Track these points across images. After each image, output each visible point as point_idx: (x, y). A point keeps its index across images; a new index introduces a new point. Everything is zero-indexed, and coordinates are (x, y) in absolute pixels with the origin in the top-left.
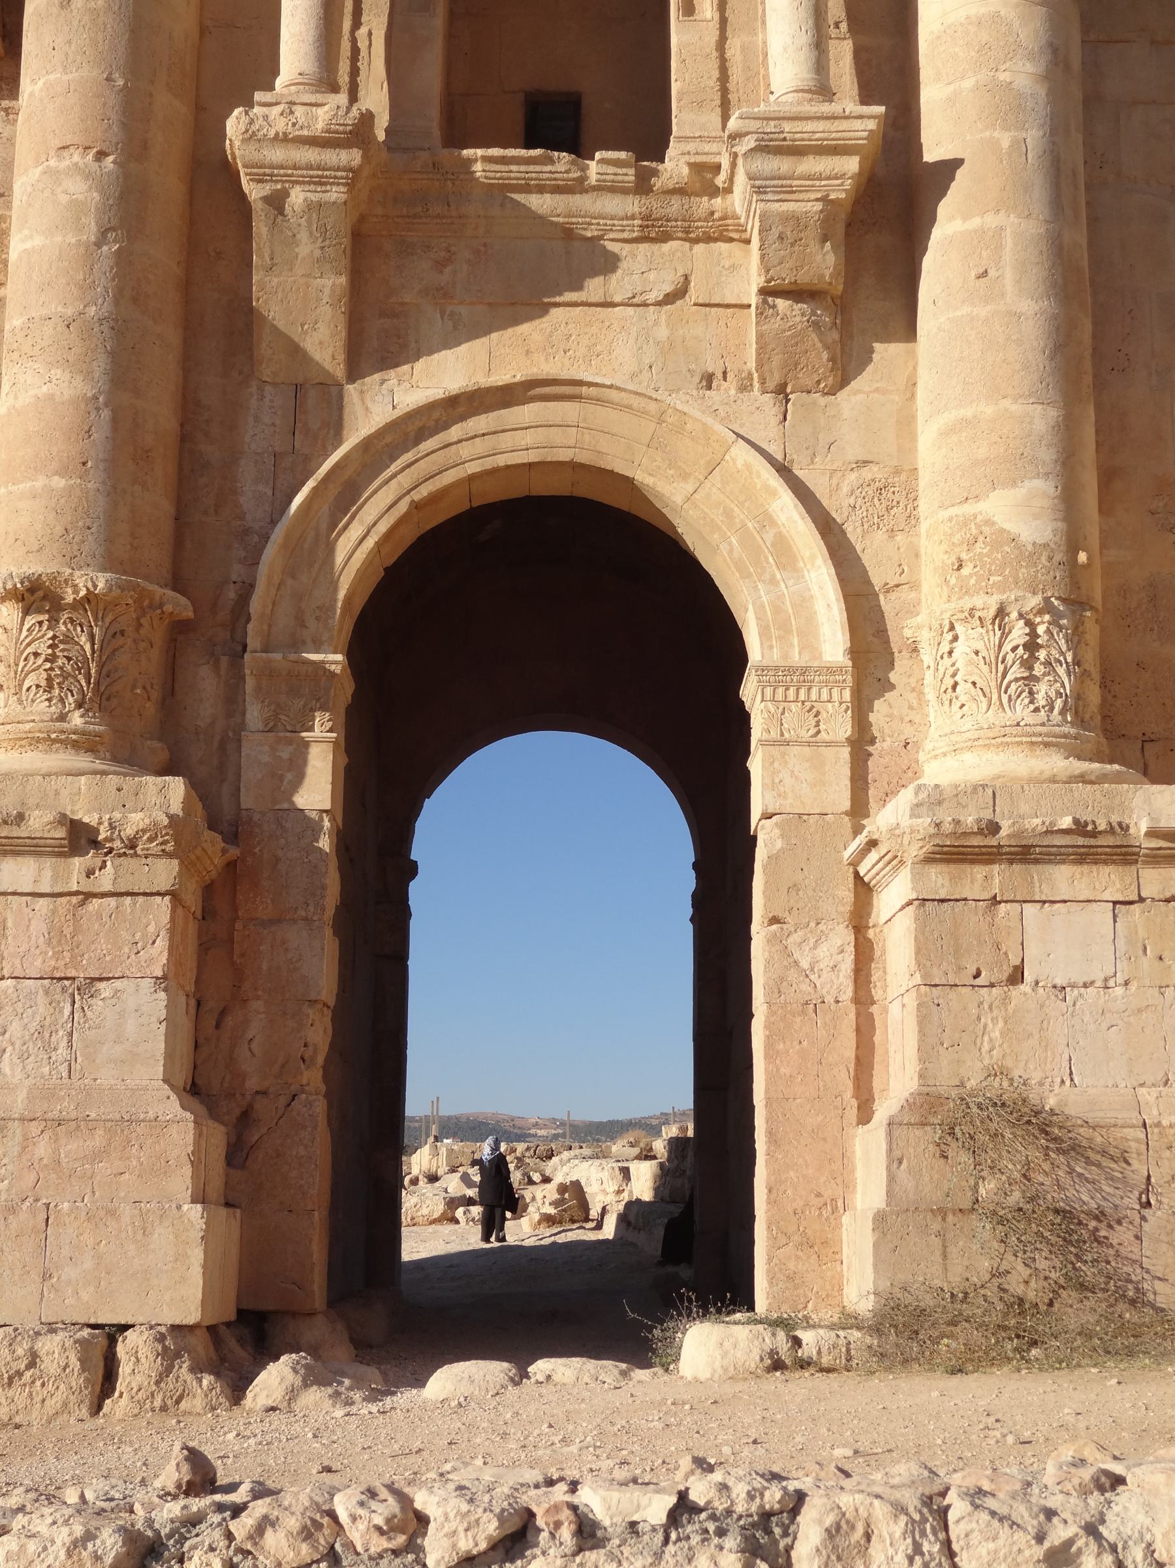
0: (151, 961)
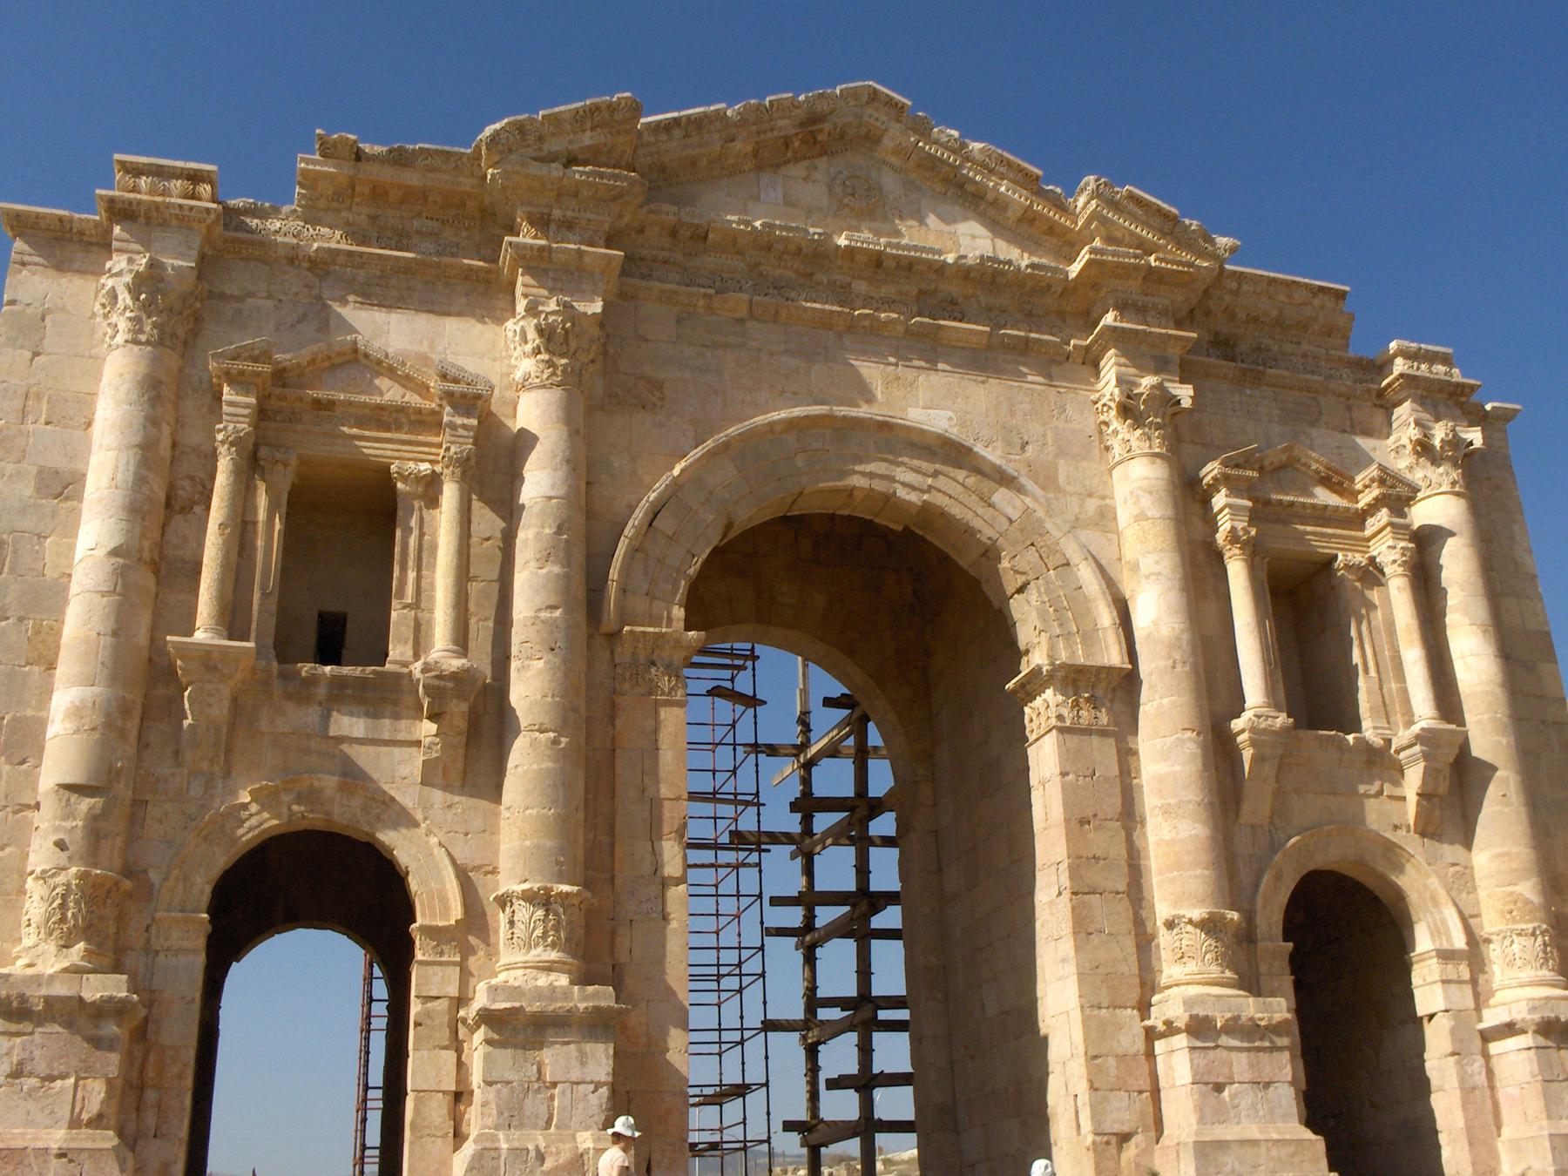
0: (1287, 1074)
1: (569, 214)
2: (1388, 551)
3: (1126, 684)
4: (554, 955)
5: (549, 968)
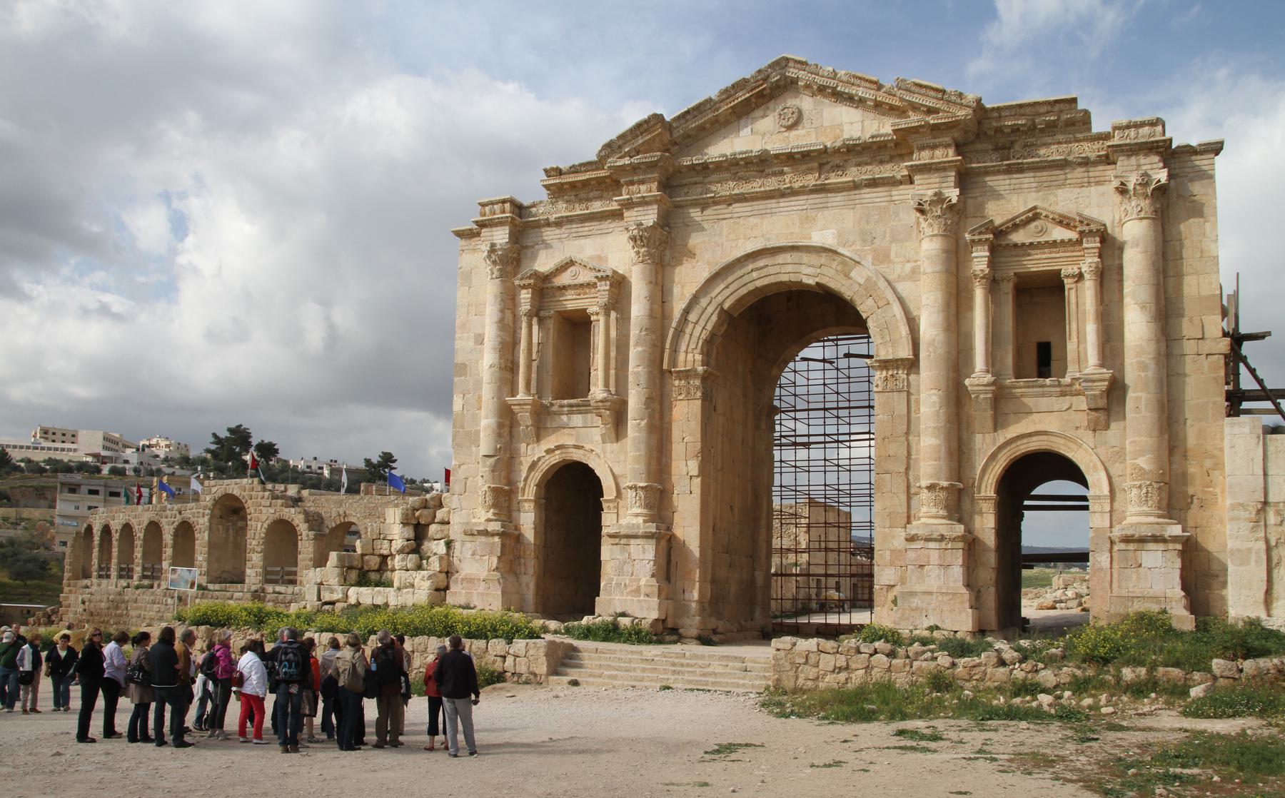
1: (641, 177)
2: (1088, 263)
3: (912, 365)
4: (639, 511)
5: (637, 515)
